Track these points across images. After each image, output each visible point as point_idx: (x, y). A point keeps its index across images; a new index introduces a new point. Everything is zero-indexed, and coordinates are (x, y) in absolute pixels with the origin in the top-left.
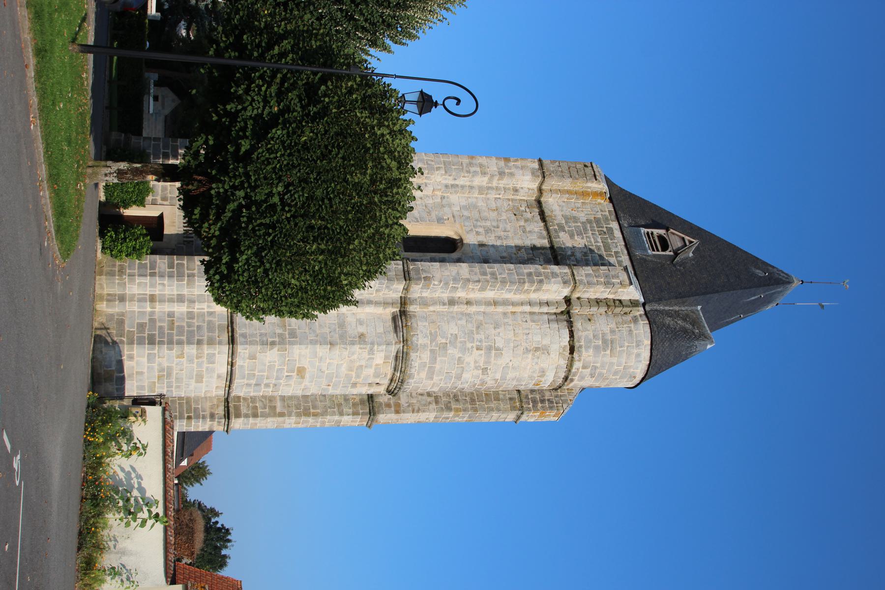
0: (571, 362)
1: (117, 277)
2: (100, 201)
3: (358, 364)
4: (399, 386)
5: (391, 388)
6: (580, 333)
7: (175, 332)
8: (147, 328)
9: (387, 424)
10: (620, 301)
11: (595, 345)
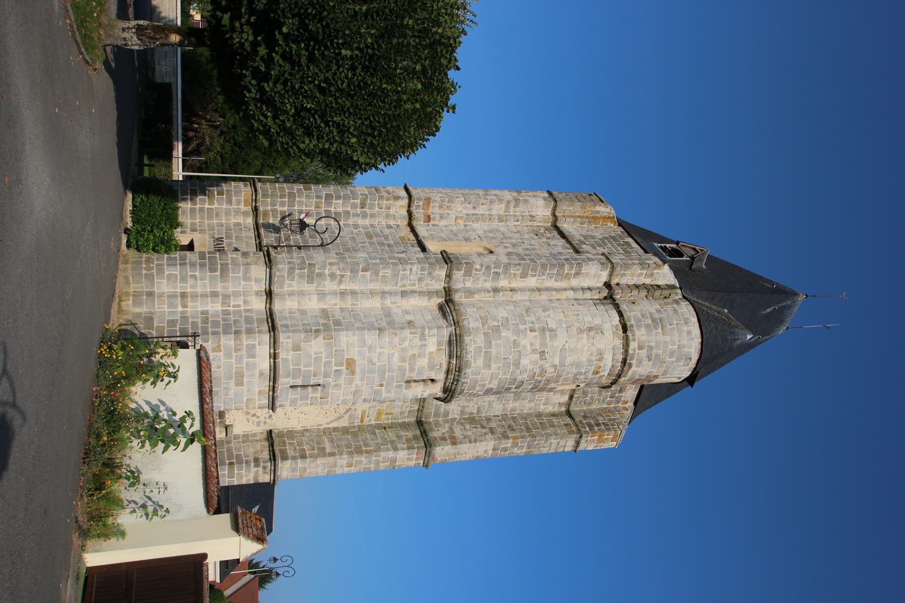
0: (626, 345)
1: (144, 266)
3: (410, 353)
4: (456, 378)
5: (447, 384)
6: (628, 314)
7: (209, 325)
8: (179, 323)
10: (658, 286)
11: (645, 324)
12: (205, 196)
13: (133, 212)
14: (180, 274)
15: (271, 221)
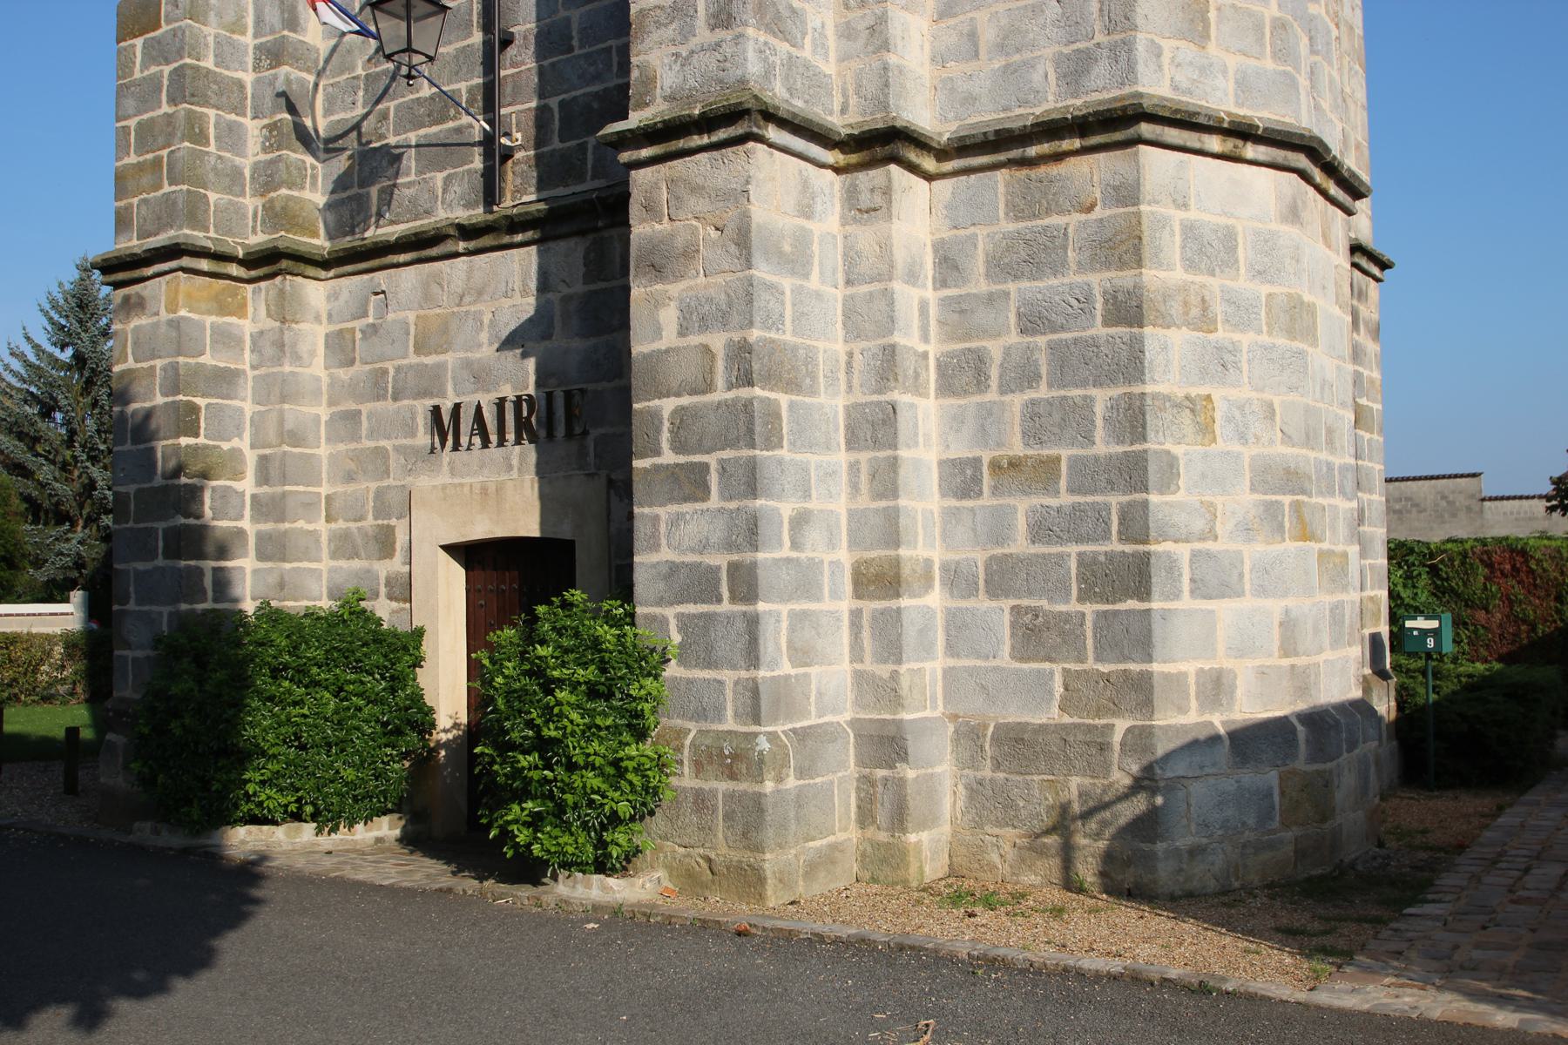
1: (769, 786)
2: (400, 840)
7: (1065, 453)
8: (1044, 603)
12: (201, 489)
13: (326, 818)
14: (789, 599)
15: (320, 199)
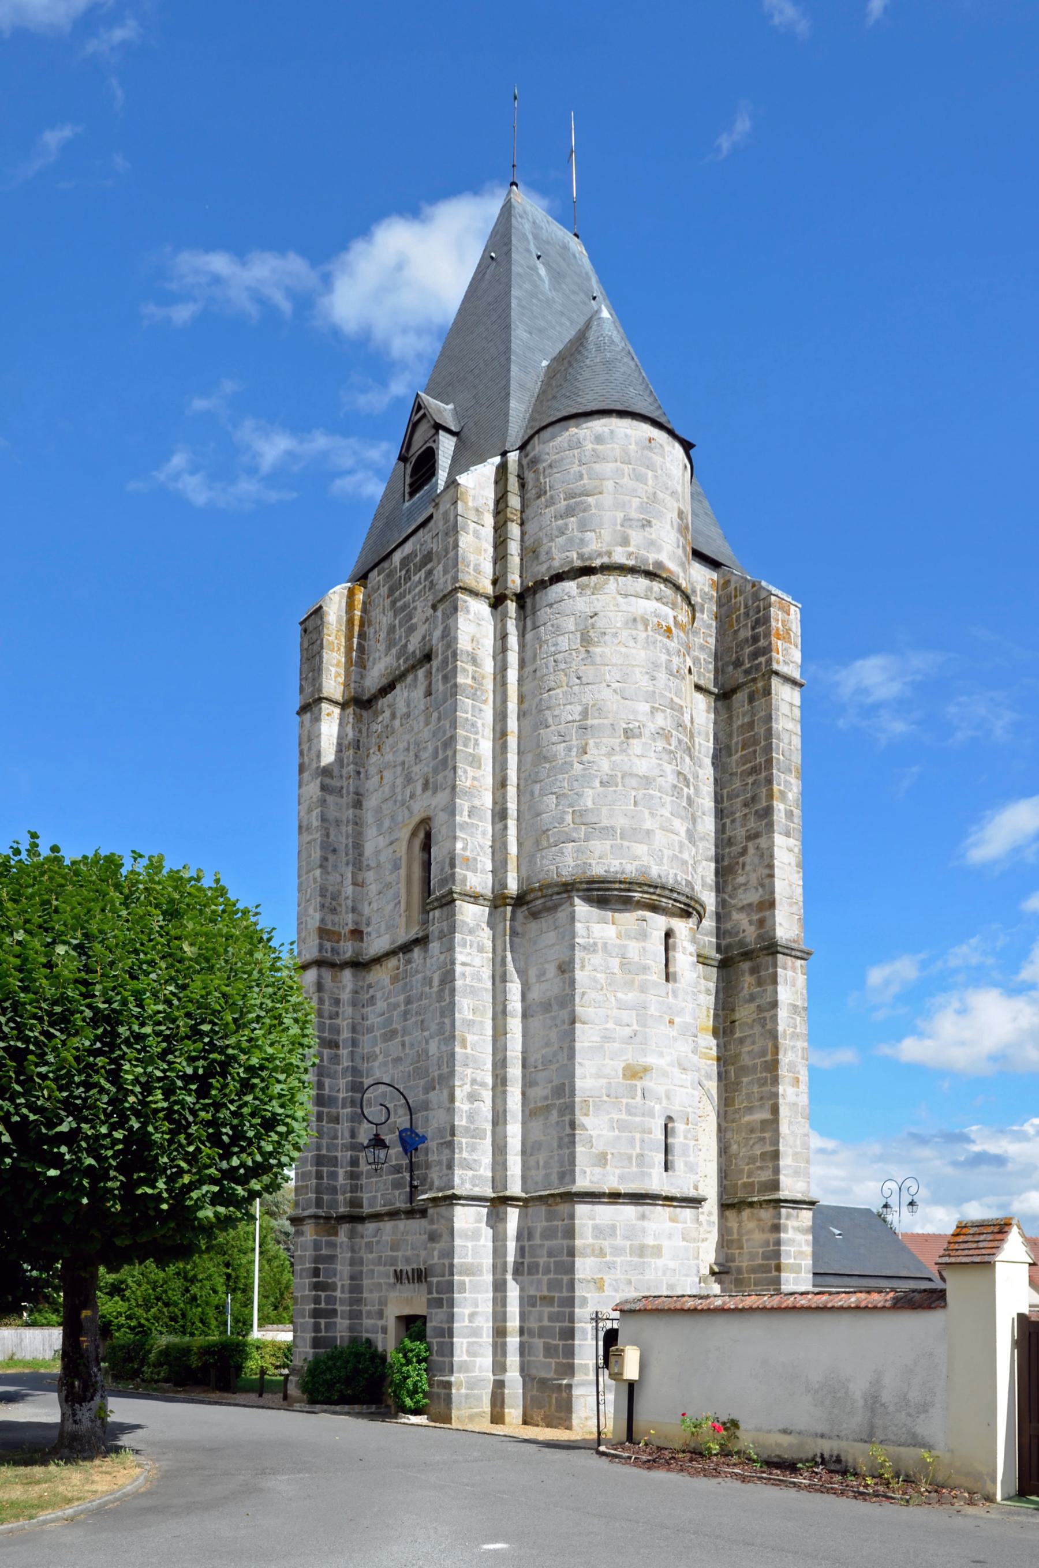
7: (557, 1295)
9: (807, 922)
